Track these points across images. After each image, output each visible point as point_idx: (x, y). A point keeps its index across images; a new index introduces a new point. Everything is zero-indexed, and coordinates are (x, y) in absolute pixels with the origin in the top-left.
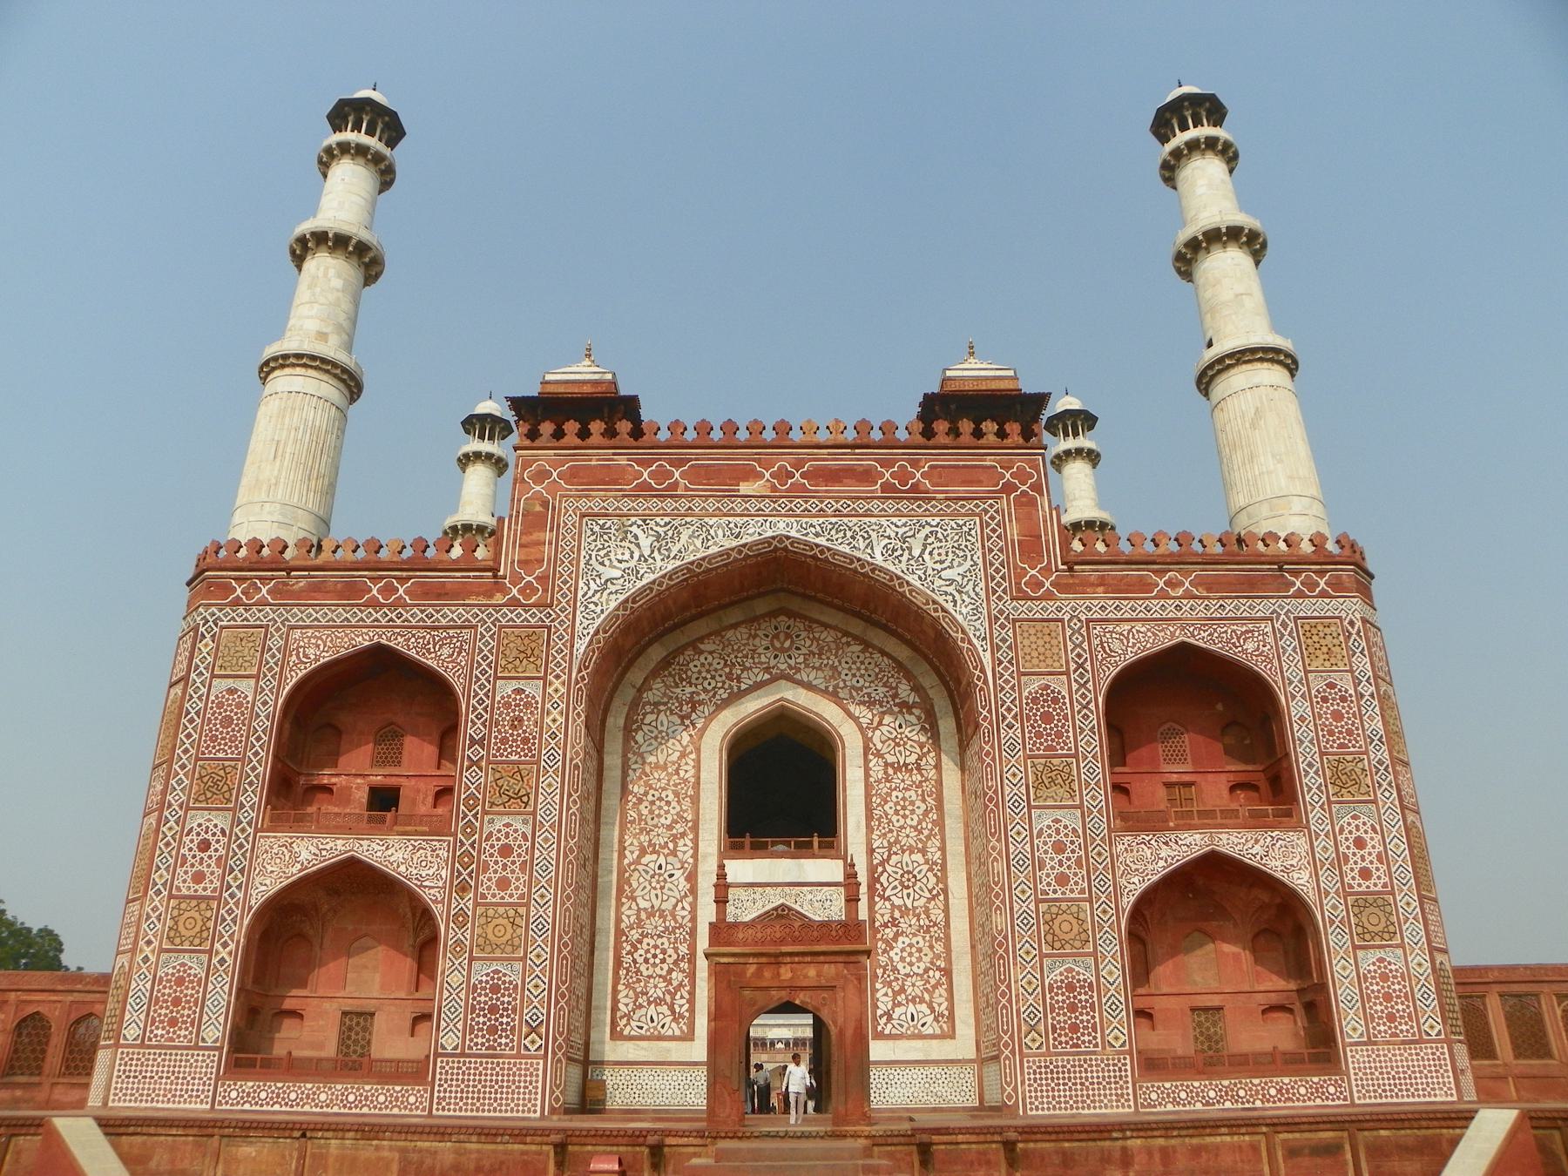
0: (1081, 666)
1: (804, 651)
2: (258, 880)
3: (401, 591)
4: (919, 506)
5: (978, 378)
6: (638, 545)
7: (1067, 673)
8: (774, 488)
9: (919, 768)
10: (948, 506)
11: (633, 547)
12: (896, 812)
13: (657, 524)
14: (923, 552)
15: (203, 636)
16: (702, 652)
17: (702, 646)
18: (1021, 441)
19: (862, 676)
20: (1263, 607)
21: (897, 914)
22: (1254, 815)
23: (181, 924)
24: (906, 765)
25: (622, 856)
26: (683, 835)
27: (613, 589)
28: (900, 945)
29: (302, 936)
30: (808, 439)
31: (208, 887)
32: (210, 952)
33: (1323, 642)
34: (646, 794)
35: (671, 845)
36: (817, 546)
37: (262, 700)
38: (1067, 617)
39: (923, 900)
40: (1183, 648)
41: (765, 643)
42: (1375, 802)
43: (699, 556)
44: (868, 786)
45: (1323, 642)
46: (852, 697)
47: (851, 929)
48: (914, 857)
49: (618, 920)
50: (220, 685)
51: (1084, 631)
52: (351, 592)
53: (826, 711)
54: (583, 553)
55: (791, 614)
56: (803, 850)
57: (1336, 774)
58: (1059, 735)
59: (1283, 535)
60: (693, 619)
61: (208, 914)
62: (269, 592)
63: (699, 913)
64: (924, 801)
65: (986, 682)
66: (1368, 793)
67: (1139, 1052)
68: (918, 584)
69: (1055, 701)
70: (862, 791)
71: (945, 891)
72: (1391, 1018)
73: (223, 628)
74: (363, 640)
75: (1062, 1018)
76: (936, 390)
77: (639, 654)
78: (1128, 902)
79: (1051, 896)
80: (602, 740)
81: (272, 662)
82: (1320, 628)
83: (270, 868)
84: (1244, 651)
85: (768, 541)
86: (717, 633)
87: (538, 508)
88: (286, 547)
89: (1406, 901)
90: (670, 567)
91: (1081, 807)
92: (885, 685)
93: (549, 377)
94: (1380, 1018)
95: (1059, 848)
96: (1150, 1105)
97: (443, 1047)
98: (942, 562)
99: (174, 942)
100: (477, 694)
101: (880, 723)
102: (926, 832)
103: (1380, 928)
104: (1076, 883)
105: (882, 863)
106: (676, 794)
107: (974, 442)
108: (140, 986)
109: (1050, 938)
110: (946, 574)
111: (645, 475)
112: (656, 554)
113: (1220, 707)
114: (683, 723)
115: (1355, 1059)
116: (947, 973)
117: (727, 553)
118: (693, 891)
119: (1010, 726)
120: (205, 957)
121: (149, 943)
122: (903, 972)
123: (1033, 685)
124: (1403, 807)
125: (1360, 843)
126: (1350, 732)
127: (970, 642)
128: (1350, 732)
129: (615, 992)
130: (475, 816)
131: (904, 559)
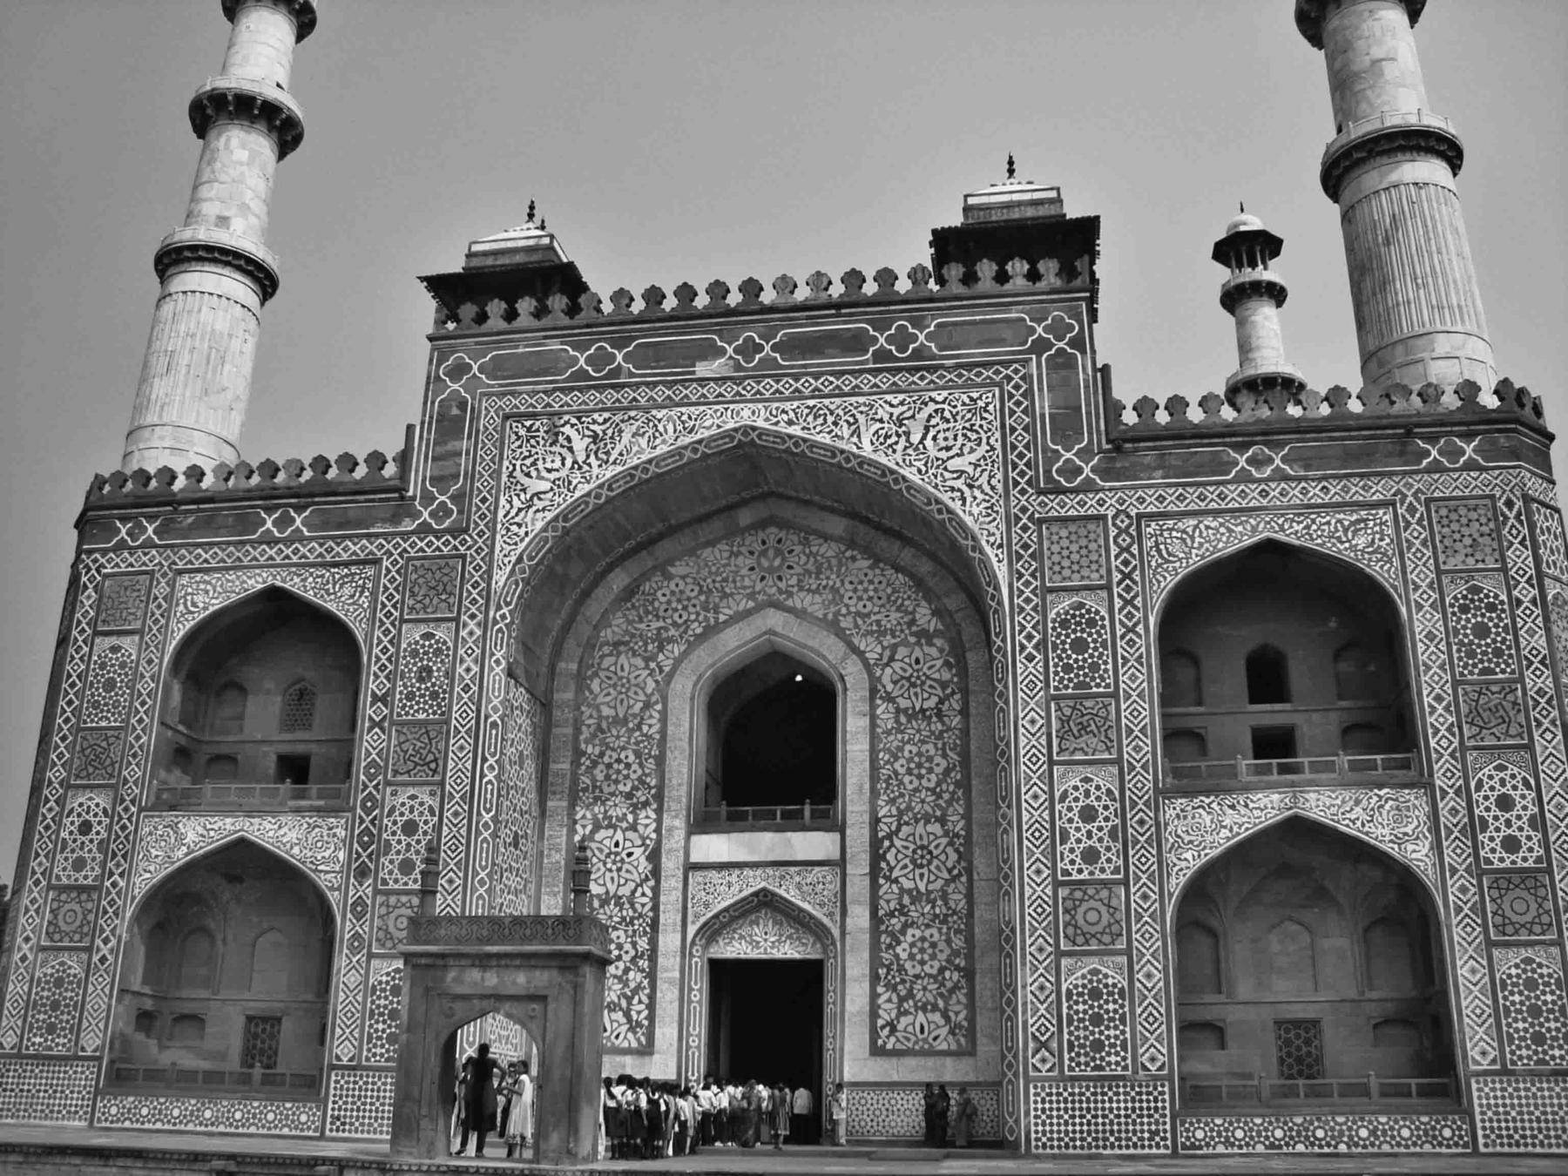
0: (1126, 576)
1: (798, 570)
2: (143, 865)
3: (298, 522)
4: (922, 378)
5: (1009, 206)
6: (571, 449)
7: (1108, 588)
8: (738, 367)
9: (940, 715)
10: (960, 376)
11: (564, 451)
12: (909, 772)
13: (594, 422)
14: (924, 437)
15: (86, 587)
16: (669, 577)
17: (672, 570)
18: (1058, 283)
19: (870, 599)
20: (1379, 490)
21: (906, 900)
23: (60, 917)
24: (923, 711)
25: (572, 831)
26: (646, 804)
27: (540, 505)
28: (909, 939)
29: (204, 931)
30: (783, 301)
31: (88, 876)
32: (89, 950)
33: (1465, 531)
34: (602, 754)
35: (630, 818)
36: (790, 437)
37: (145, 659)
38: (1110, 513)
39: (940, 883)
40: (1269, 548)
41: (750, 562)
42: (1530, 747)
43: (644, 458)
45: (1465, 531)
46: (857, 626)
47: (574, 923)
48: (930, 828)
50: (103, 643)
51: (1132, 530)
53: (825, 650)
54: (506, 463)
55: (783, 525)
56: (793, 822)
57: (1475, 711)
58: (1094, 667)
59: (1416, 388)
60: (661, 536)
61: (89, 906)
62: (264, 522)
63: (662, 899)
64: (945, 756)
65: (1000, 603)
66: (1520, 735)
67: (1182, 1079)
68: (916, 479)
69: (1091, 623)
70: (867, 747)
71: (969, 871)
73: (106, 576)
74: (256, 582)
75: (1082, 1033)
77: (595, 584)
78: (1176, 884)
79: (1076, 876)
80: (549, 692)
81: (158, 613)
82: (1462, 511)
83: (154, 853)
84: (1354, 548)
85: (729, 435)
86: (692, 552)
87: (455, 411)
88: (174, 477)
90: (609, 475)
91: (1118, 761)
92: (898, 610)
93: (475, 248)
94: (1523, 1039)
95: (1088, 814)
96: (1193, 1146)
97: (338, 1058)
98: (948, 449)
100: (380, 642)
101: (892, 659)
102: (946, 796)
103: (1528, 918)
104: (1109, 860)
105: (889, 837)
106: (638, 754)
107: (997, 288)
109: (1070, 930)
110: (951, 465)
111: (582, 361)
112: (592, 459)
113: (1333, 624)
114: (647, 667)
116: (969, 974)
117: (678, 452)
118: (656, 873)
119: (1030, 658)
120: (84, 956)
121: (27, 939)
122: (911, 972)
123: (1060, 606)
125: (1505, 803)
126: (1498, 653)
127: (982, 552)
128: (1498, 653)
130: (376, 787)
131: (899, 447)
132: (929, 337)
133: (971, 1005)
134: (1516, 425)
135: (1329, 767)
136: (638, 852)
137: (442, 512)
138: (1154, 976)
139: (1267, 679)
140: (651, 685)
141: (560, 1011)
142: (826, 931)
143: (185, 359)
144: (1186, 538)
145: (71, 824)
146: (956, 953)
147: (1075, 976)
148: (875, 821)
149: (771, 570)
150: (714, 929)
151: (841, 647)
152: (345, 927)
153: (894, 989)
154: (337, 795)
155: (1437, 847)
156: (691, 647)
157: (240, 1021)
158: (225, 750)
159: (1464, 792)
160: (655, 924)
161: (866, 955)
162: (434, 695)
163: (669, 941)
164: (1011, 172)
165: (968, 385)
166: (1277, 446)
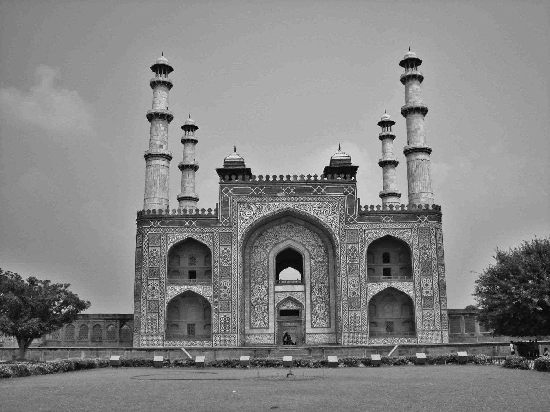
8: (286, 194)
9: (323, 262)
20: (409, 226)
22: (401, 278)
25: (250, 285)
29: (176, 307)
31: (156, 298)
40: (388, 235)
41: (285, 229)
42: (432, 275)
44: (310, 267)
49: (250, 301)
52: (181, 223)
53: (300, 248)
55: (291, 222)
57: (423, 268)
58: (355, 258)
68: (322, 220)
69: (355, 250)
71: (329, 293)
72: (429, 325)
74: (186, 236)
76: (329, 165)
78: (369, 298)
89: (436, 299)
91: (359, 276)
93: (226, 160)
95: (354, 286)
99: (150, 311)
106: (263, 269)
108: (143, 321)
110: (330, 217)
113: (399, 248)
115: (419, 334)
116: (329, 312)
117: (275, 212)
118: (268, 293)
123: (349, 246)
124: (439, 276)
125: (427, 285)
128: (428, 258)
129: (250, 317)
132: (325, 190)
133: (330, 319)
134: (435, 213)
135: (396, 278)
136: (264, 289)
137: (226, 223)
138: (365, 314)
139: (386, 259)
140: (265, 255)
141: (299, 328)
142: (302, 304)
143: (158, 182)
144: (373, 234)
145: (150, 288)
146: (327, 309)
147: (351, 314)
148: (311, 283)
149: (289, 232)
150: (280, 304)
151: (304, 248)
152: (213, 307)
153: (315, 315)
154: (209, 281)
155: (415, 293)
156: (273, 247)
157: (186, 326)
158: (175, 269)
159: (420, 283)
160: (268, 304)
161: (310, 309)
162: (228, 261)
163: (272, 307)
164: (339, 149)
165: (332, 201)
166: (390, 216)
